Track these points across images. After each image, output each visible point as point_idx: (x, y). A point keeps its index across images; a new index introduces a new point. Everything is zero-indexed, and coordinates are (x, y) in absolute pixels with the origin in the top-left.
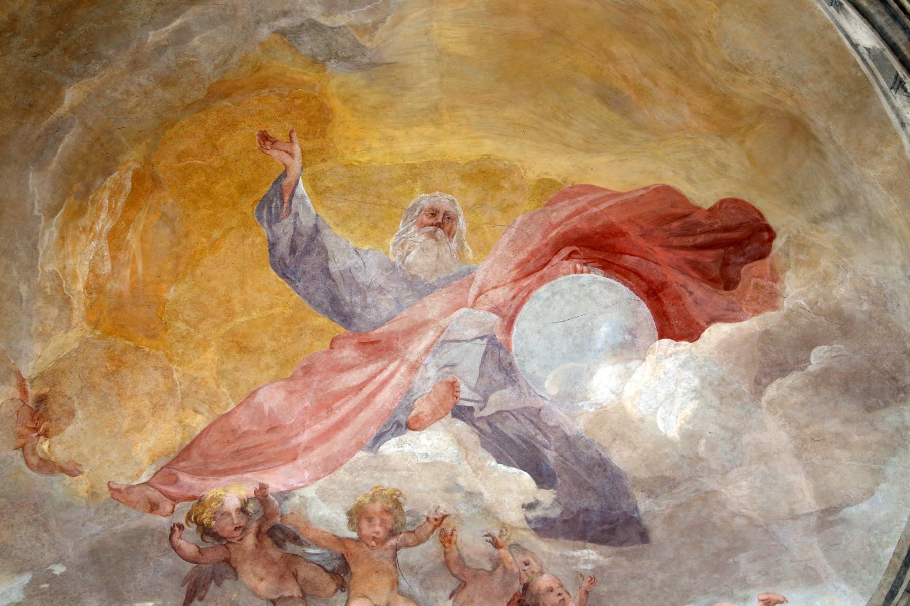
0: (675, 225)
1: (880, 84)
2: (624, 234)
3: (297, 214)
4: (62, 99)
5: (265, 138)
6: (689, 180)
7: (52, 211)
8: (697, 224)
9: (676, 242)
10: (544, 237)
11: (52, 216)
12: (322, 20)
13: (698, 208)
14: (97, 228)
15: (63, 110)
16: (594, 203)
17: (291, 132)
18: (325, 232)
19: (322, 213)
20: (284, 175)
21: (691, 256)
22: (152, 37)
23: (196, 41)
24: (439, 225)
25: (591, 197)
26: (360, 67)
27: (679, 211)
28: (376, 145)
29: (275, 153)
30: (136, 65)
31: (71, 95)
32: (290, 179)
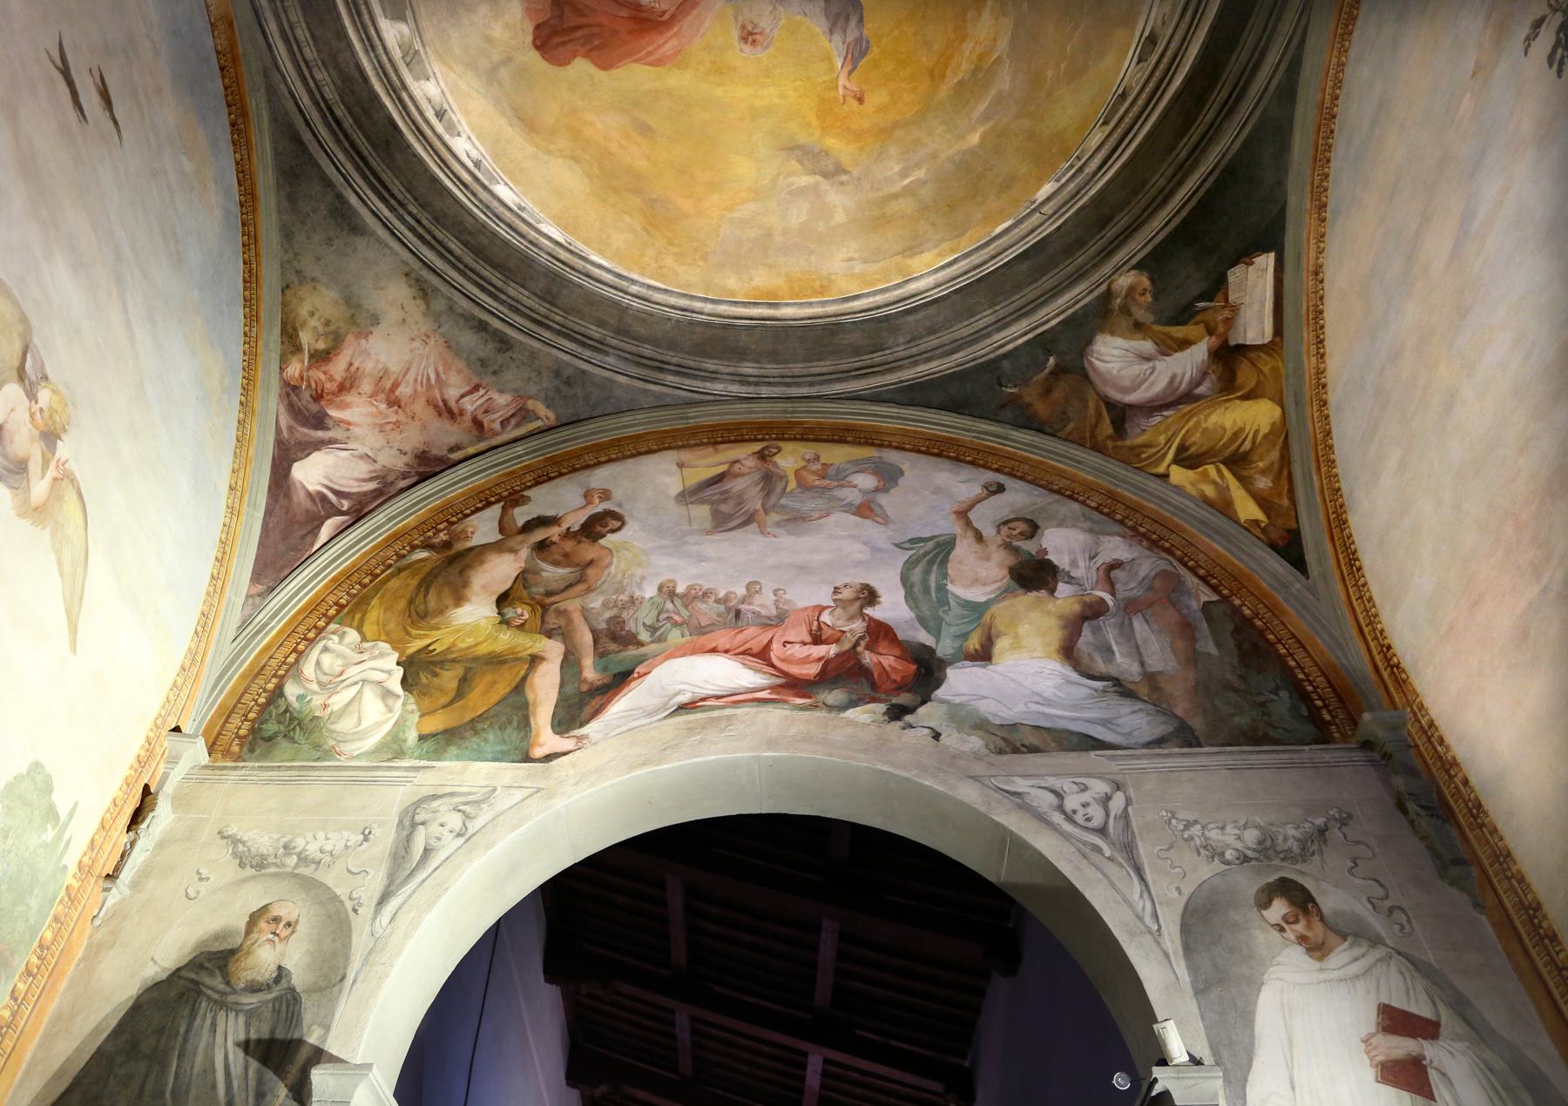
0: (596, 43)
1: (488, 163)
2: (630, 33)
3: (843, 43)
4: (980, 138)
5: (861, 100)
6: (591, 76)
7: (999, 60)
8: (583, 45)
9: (595, 30)
10: (681, 27)
11: (999, 57)
12: (819, 178)
13: (583, 56)
14: (972, 44)
15: (981, 130)
16: (650, 53)
17: (844, 103)
18: (826, 29)
19: (827, 44)
20: (850, 73)
21: (585, 21)
22: (921, 174)
23: (897, 168)
24: (751, 34)
25: (652, 58)
26: (799, 147)
27: (595, 53)
28: (790, 93)
29: (855, 89)
30: (934, 156)
31: (974, 139)
32: (846, 70)
